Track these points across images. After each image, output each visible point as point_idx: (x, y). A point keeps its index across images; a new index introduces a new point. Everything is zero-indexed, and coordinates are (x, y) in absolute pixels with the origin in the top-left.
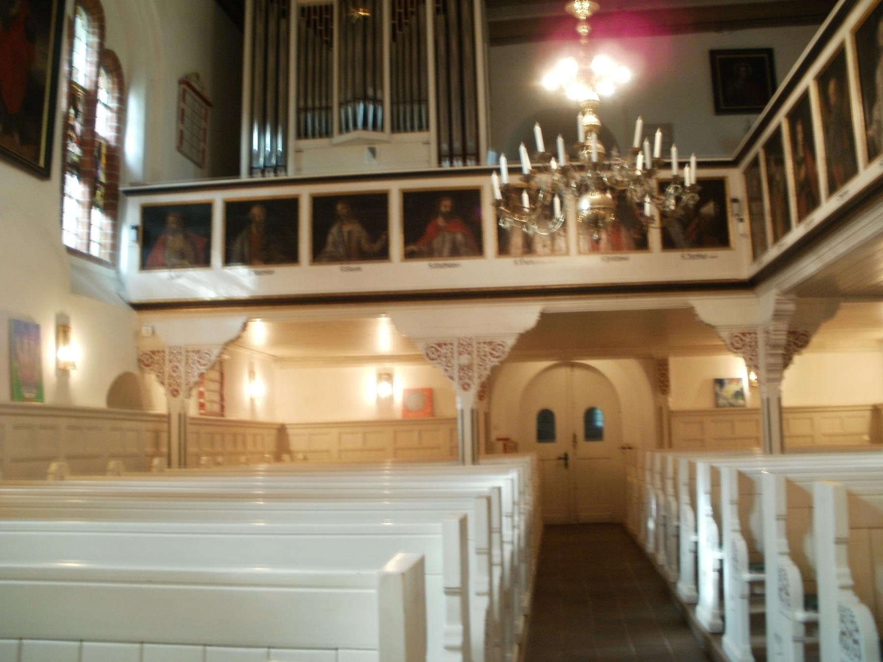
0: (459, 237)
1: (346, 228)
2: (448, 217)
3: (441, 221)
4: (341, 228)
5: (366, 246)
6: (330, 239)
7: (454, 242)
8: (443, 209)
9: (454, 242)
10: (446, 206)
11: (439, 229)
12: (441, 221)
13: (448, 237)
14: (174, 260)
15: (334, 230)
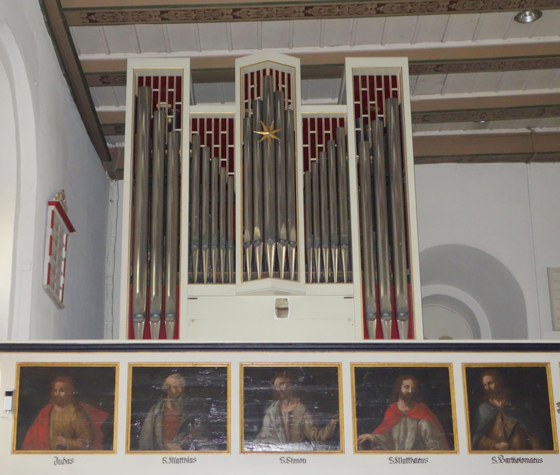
0: (424, 425)
1: (285, 410)
2: (409, 400)
3: (401, 406)
4: (280, 407)
5: (312, 433)
6: (266, 420)
7: (418, 430)
8: (404, 390)
9: (418, 430)
10: (407, 387)
11: (399, 415)
12: (401, 406)
13: (411, 424)
14: (62, 440)
15: (271, 410)
